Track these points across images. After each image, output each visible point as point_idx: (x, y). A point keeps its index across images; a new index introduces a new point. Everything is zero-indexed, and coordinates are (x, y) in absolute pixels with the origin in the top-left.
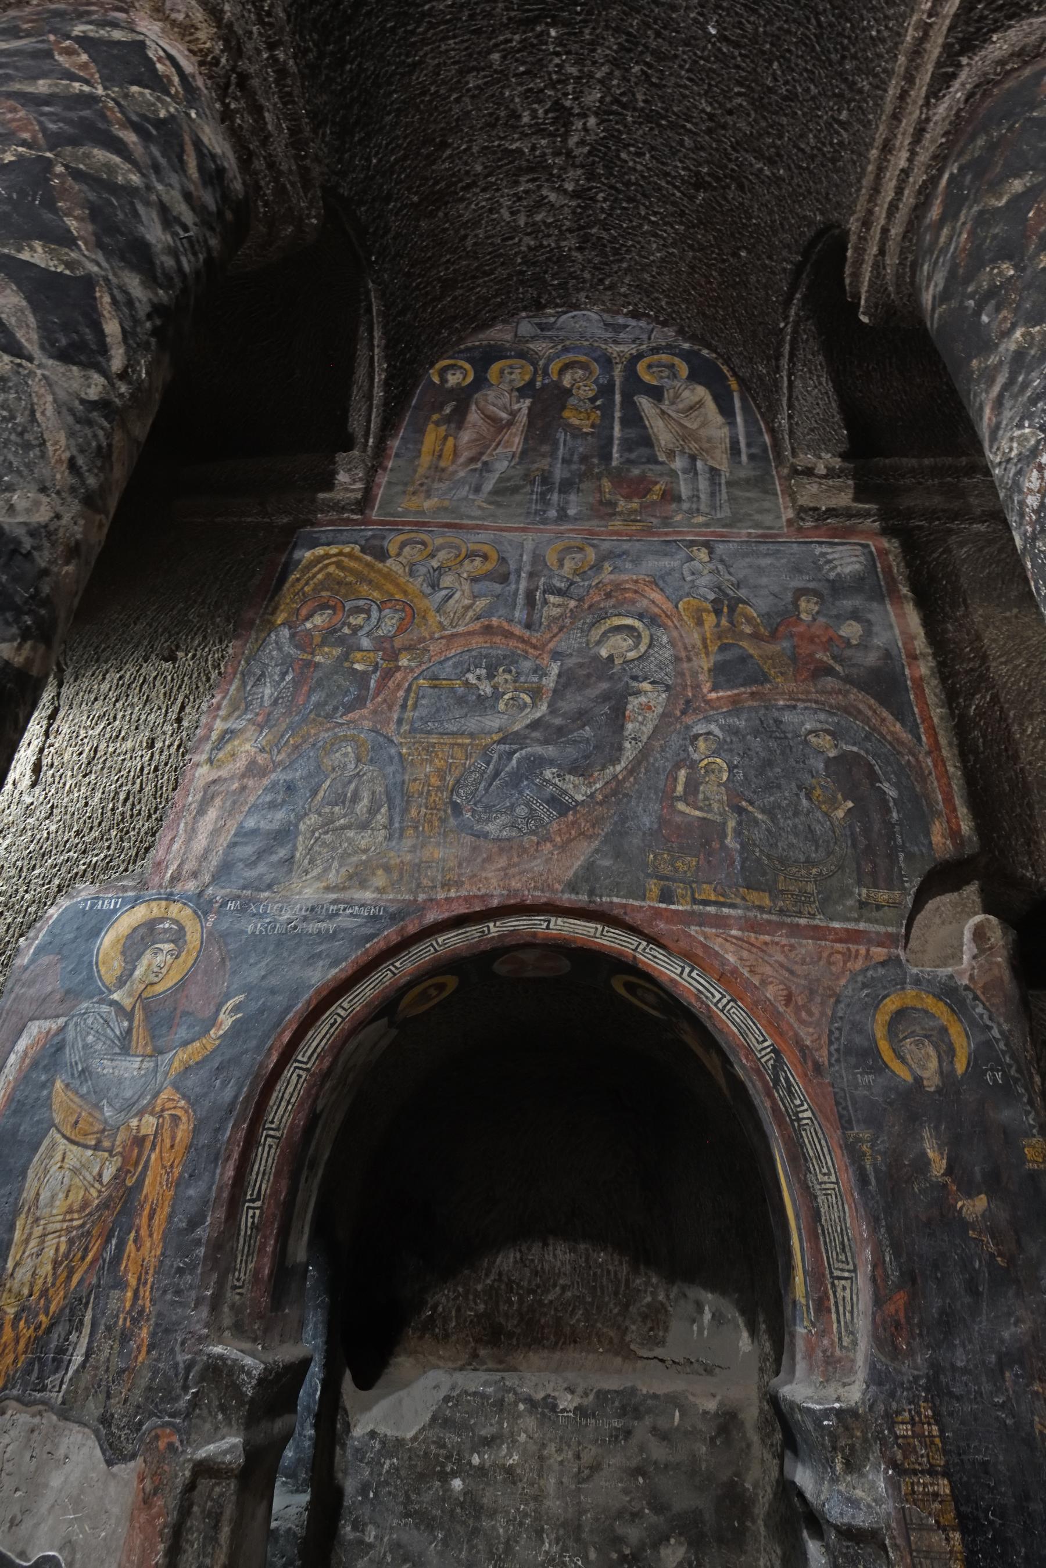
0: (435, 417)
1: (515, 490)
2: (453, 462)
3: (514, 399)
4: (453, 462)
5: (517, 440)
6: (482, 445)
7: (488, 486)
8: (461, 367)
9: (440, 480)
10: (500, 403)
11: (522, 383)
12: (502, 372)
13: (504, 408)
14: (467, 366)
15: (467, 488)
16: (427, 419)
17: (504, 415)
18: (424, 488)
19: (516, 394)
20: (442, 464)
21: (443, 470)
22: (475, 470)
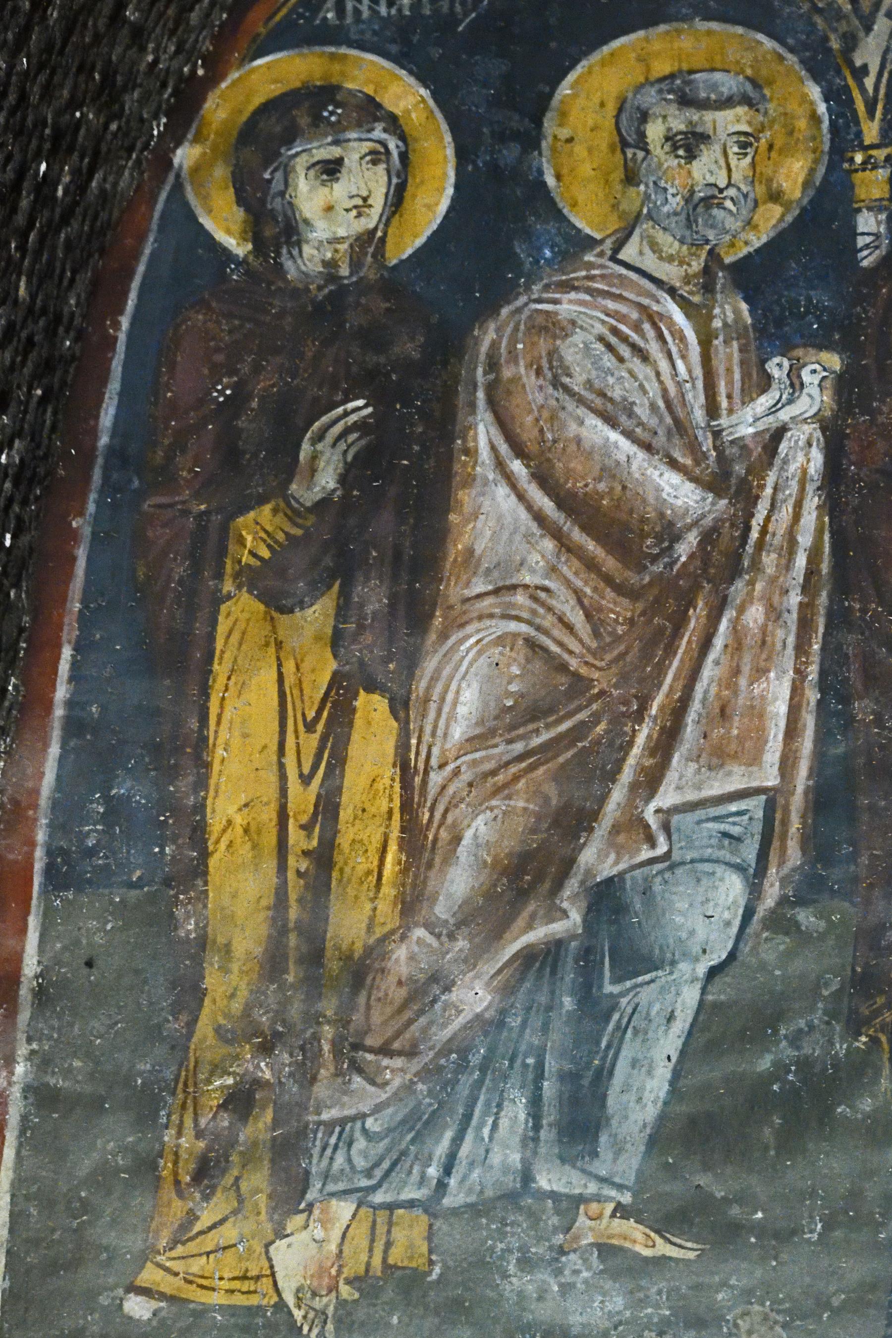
0: (256, 532)
1: (808, 1104)
2: (411, 904)
3: (729, 354)
4: (411, 904)
5: (777, 692)
6: (577, 743)
7: (643, 1090)
8: (370, 110)
9: (352, 1054)
10: (639, 386)
11: (771, 219)
12: (629, 137)
13: (673, 436)
14: (406, 95)
15: (517, 1110)
16: (209, 547)
17: (677, 492)
18: (261, 1126)
19: (731, 309)
20: (350, 923)
21: (361, 971)
22: (541, 961)
